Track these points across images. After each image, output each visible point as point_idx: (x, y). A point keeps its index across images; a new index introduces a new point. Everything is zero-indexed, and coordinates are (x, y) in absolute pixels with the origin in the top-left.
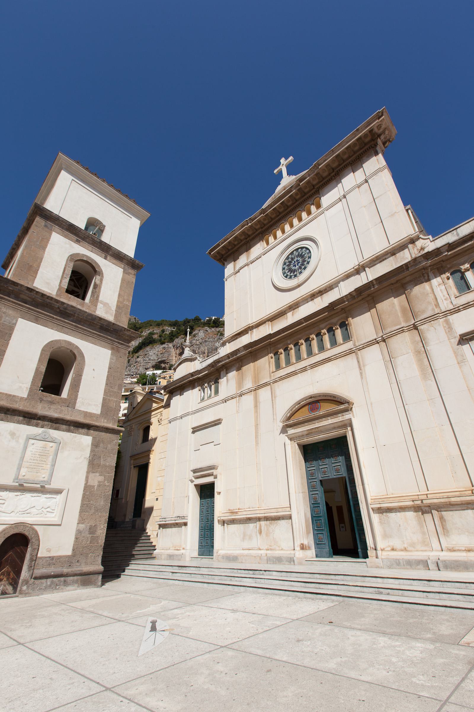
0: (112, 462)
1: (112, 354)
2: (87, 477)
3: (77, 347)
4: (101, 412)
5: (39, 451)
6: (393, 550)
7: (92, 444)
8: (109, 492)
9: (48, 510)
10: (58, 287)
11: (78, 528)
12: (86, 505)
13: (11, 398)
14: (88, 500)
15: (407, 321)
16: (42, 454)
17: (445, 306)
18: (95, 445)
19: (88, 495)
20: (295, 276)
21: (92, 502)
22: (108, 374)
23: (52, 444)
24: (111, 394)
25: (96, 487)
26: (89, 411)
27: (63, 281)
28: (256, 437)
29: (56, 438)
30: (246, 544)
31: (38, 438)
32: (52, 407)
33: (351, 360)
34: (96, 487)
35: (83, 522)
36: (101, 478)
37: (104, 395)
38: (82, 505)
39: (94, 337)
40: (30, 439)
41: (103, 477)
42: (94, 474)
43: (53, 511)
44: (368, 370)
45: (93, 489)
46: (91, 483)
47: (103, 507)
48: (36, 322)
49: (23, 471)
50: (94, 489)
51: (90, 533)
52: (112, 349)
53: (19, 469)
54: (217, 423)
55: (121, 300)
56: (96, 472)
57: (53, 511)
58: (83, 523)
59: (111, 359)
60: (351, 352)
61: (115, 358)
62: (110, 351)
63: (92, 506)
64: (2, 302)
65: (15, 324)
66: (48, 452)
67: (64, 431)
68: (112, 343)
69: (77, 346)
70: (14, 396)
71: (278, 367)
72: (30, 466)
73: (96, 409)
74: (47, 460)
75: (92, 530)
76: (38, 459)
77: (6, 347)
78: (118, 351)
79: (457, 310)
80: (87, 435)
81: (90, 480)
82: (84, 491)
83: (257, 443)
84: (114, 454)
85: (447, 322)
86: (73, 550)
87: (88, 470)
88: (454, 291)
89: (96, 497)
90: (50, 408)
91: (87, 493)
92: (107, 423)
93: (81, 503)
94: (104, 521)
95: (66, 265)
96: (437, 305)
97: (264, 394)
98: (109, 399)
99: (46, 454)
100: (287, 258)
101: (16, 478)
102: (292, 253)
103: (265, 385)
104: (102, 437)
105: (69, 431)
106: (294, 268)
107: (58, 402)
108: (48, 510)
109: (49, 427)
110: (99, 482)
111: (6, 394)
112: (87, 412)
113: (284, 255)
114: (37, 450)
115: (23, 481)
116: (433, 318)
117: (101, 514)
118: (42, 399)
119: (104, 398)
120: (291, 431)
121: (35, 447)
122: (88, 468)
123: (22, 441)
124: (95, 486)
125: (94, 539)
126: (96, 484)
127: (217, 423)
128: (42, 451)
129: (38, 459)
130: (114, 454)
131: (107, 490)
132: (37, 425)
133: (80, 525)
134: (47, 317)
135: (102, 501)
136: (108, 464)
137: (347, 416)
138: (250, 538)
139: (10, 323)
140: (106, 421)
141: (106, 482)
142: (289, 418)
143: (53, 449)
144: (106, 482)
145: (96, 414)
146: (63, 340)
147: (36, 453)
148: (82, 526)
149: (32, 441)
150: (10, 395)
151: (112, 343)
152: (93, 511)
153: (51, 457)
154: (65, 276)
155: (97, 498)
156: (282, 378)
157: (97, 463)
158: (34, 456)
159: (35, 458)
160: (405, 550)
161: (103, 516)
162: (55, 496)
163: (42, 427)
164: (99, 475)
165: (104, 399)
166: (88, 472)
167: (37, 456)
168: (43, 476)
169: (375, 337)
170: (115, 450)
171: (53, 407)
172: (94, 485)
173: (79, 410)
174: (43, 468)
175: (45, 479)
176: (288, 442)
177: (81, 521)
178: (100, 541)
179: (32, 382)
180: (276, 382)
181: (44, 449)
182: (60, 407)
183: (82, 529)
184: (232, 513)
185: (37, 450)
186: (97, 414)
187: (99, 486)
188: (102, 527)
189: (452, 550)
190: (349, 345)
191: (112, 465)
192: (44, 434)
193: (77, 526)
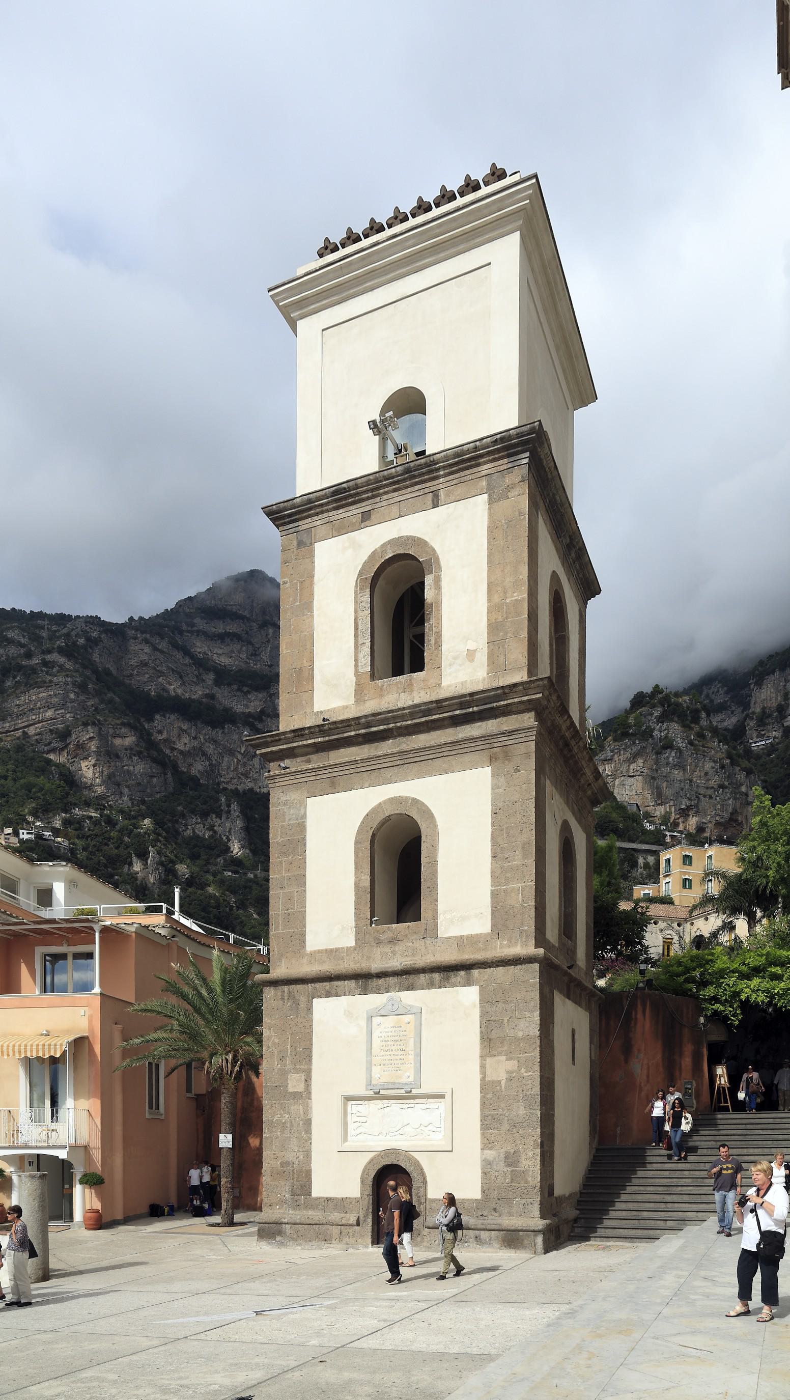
0: (530, 1028)
1: (494, 775)
2: (483, 1067)
3: (415, 801)
4: (493, 926)
5: (391, 1034)
7: (482, 1002)
8: (534, 1090)
9: (430, 1128)
10: (354, 679)
11: (484, 1157)
12: (490, 1117)
13: (334, 954)
14: (493, 1108)
16: (396, 1038)
18: (486, 1001)
19: (491, 1099)
21: (501, 1110)
22: (493, 832)
23: (407, 1018)
24: (508, 875)
25: (503, 1083)
26: (465, 933)
27: (361, 655)
29: (411, 1006)
31: (382, 1012)
32: (397, 949)
34: (503, 1083)
35: (490, 1146)
36: (512, 1065)
37: (492, 886)
38: (483, 1119)
39: (445, 754)
40: (373, 1018)
41: (516, 1062)
42: (496, 1058)
43: (438, 1130)
45: (498, 1088)
46: (491, 1076)
47: (524, 1118)
48: (334, 791)
49: (376, 1072)
50: (501, 1086)
51: (508, 1166)
52: (493, 759)
53: (369, 1070)
55: (496, 599)
56: (500, 1054)
57: (438, 1130)
58: (490, 1149)
59: (494, 787)
61: (502, 781)
62: (488, 770)
63: (503, 1119)
64: (277, 784)
65: (305, 816)
66: (404, 1033)
67: (423, 989)
68: (487, 747)
69: (414, 799)
70: (337, 950)
72: (383, 1062)
73: (481, 925)
74: (406, 1047)
75: (511, 1160)
76: (393, 1048)
77: (305, 868)
78: (507, 757)
80: (468, 983)
81: (489, 1072)
82: (481, 1093)
84: (532, 1012)
86: (483, 1192)
87: (481, 1052)
89: (507, 1101)
90: (394, 953)
91: (489, 1096)
92: (509, 947)
93: (481, 1114)
94: (532, 1143)
95: (356, 612)
98: (505, 890)
99: (403, 1038)
101: (369, 1083)
104: (498, 982)
105: (431, 985)
107: (406, 936)
108: (430, 1128)
109: (397, 988)
110: (508, 1072)
111: (326, 950)
112: (462, 937)
114: (388, 1034)
115: (379, 1087)
117: (524, 1131)
118: (379, 939)
119: (492, 892)
121: (384, 1027)
122: (480, 1048)
123: (363, 1023)
124: (500, 1082)
125: (516, 1176)
126: (503, 1077)
128: (396, 1034)
129: (393, 1048)
130: (532, 1012)
131: (529, 1087)
132: (377, 991)
133: (486, 1152)
134: (348, 767)
135: (522, 1107)
136: (520, 1034)
139: (297, 819)
140: (505, 943)
141: (523, 1070)
143: (412, 1025)
144: (523, 1070)
145: (481, 934)
146: (385, 802)
147: (387, 1039)
148: (490, 1154)
149: (376, 1020)
150: (331, 950)
151: (487, 747)
152: (506, 1127)
153: (412, 1042)
154: (360, 641)
155: (510, 1102)
157: (498, 1035)
158: (384, 1043)
159: (387, 1048)
161: (529, 1135)
162: (436, 1106)
163: (387, 991)
164: (507, 1060)
165: (494, 895)
166: (483, 1057)
167: (390, 1043)
168: (407, 1075)
170: (532, 1003)
171: (399, 948)
172: (500, 1079)
173: (446, 938)
174: (403, 1062)
175: (411, 1079)
177: (487, 1144)
178: (530, 1179)
179: (355, 913)
181: (397, 1029)
182: (410, 944)
183: (491, 1159)
185: (388, 1034)
186: (485, 934)
187: (510, 1080)
188: (530, 1154)
191: (531, 1034)
192: (390, 1003)
193: (482, 1154)
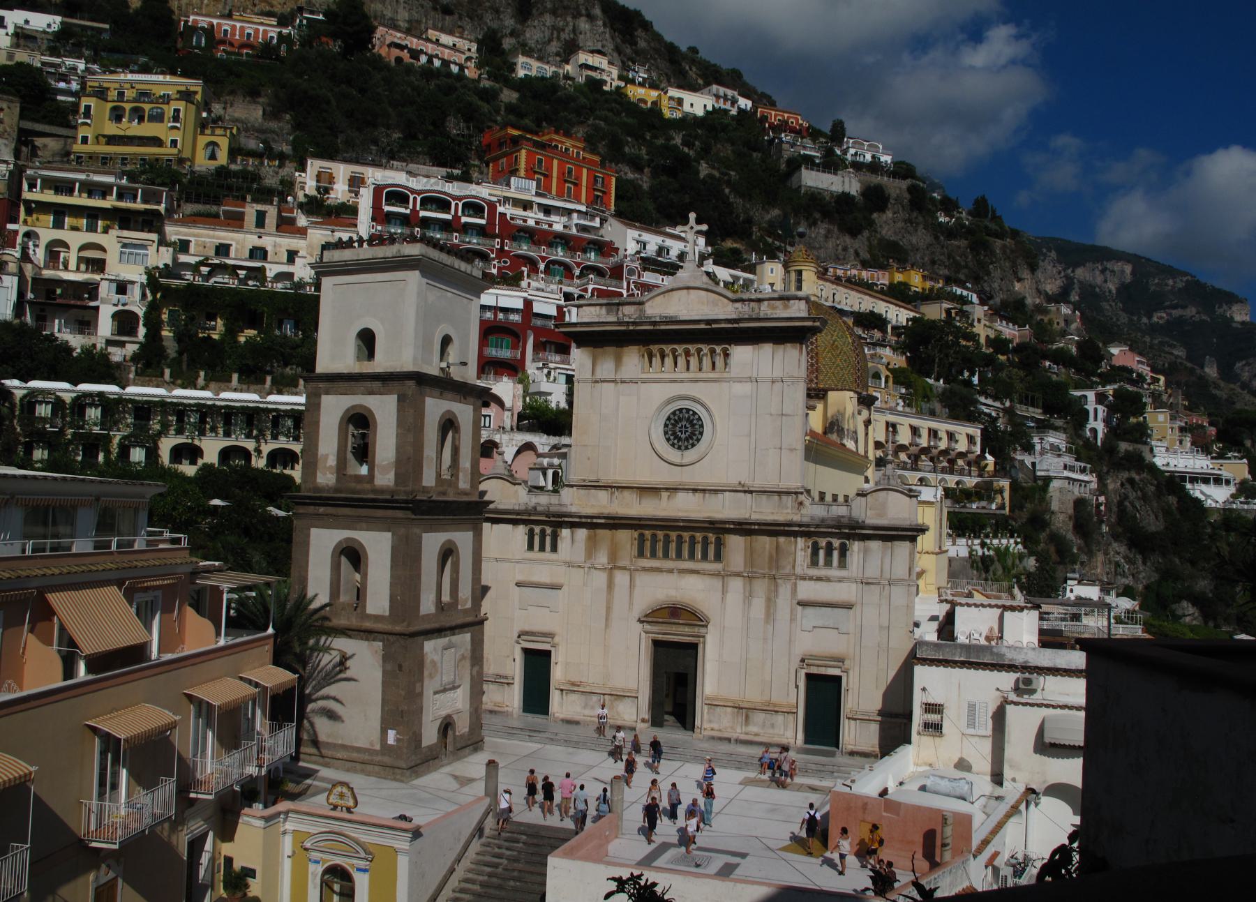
6: (712, 729)
15: (770, 569)
17: (799, 571)
20: (679, 448)
28: (607, 619)
30: (587, 712)
33: (717, 583)
44: (729, 596)
54: (556, 587)
60: (717, 574)
71: (641, 554)
79: (804, 579)
83: (607, 626)
85: (795, 584)
88: (808, 560)
96: (794, 567)
97: (621, 578)
100: (674, 413)
102: (681, 410)
103: (624, 568)
106: (679, 434)
113: (670, 406)
116: (787, 577)
120: (648, 627)
127: (556, 587)
137: (703, 630)
138: (593, 708)
142: (647, 616)
156: (644, 569)
160: (720, 730)
169: (742, 569)
176: (643, 635)
180: (637, 570)
184: (573, 684)
189: (747, 734)
190: (717, 567)
